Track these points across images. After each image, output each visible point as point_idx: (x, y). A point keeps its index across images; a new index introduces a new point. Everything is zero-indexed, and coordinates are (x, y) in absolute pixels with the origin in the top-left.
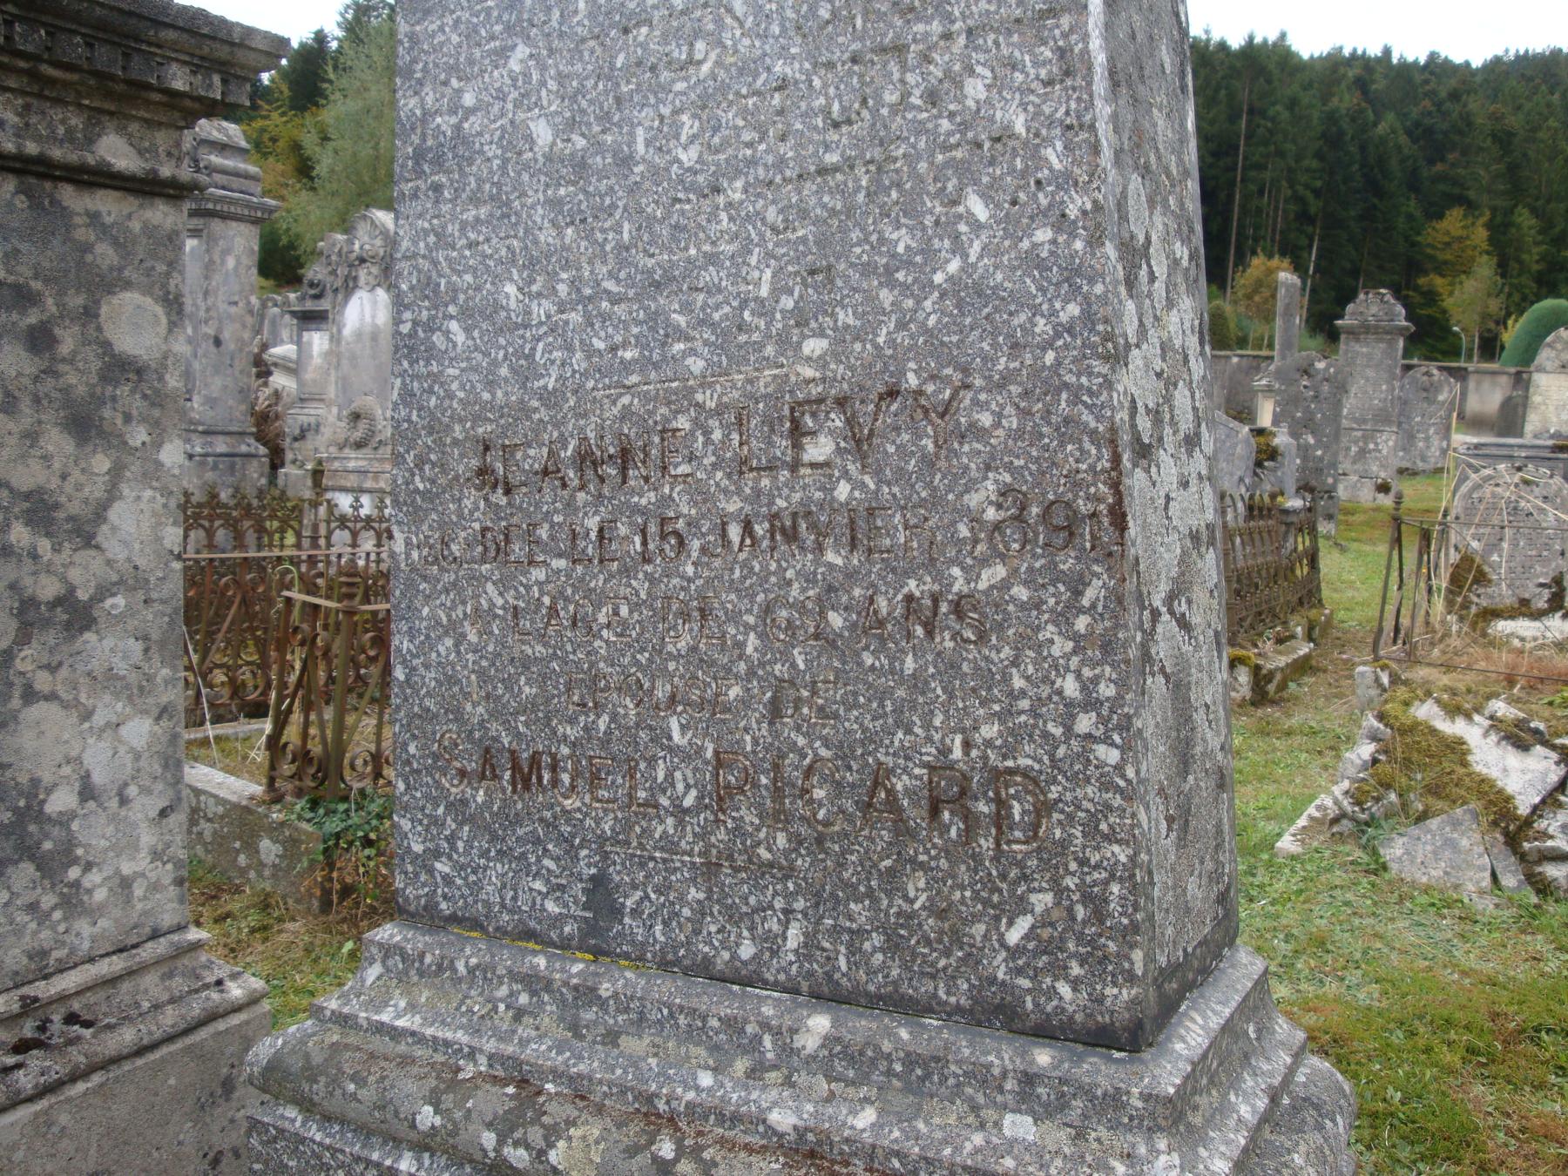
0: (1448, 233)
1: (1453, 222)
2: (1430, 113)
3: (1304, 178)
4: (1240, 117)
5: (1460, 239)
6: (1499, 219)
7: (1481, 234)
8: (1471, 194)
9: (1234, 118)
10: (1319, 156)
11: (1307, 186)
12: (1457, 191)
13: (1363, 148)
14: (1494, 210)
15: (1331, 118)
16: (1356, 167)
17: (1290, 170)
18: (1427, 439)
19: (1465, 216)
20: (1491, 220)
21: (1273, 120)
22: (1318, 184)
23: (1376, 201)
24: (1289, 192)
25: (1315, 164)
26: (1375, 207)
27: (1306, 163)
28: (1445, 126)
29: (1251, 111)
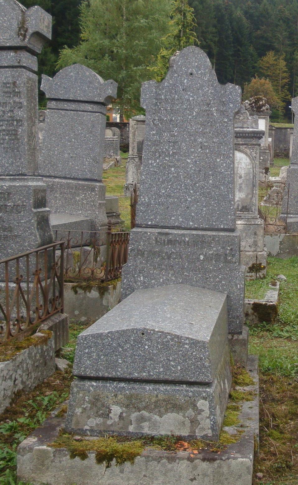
0: (268, 62)
1: (270, 57)
3: (210, 37)
5: (273, 65)
6: (289, 56)
7: (282, 64)
8: (276, 45)
10: (215, 26)
11: (211, 40)
12: (268, 44)
13: (231, 23)
14: (286, 52)
19: (275, 55)
20: (285, 57)
23: (239, 47)
25: (214, 30)
26: (239, 50)
28: (257, 14)
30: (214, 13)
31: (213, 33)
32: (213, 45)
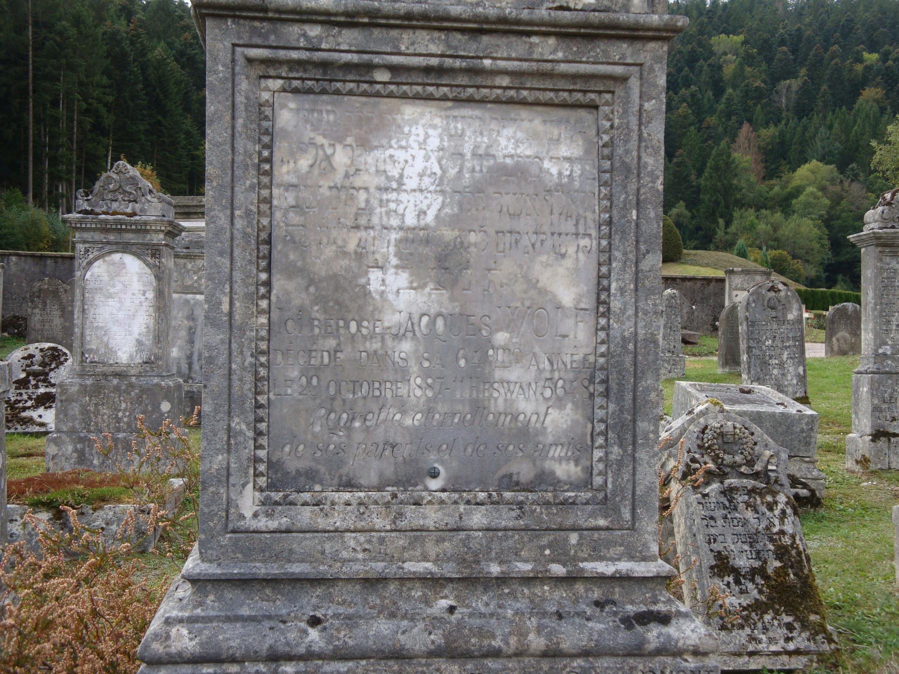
2: (191, 44)
3: (97, 93)
4: (26, 28)
9: (20, 29)
10: (107, 72)
11: (100, 101)
13: (143, 69)
15: (113, 38)
16: (141, 86)
17: (81, 84)
18: (781, 365)
21: (60, 34)
22: (110, 99)
23: (160, 118)
24: (84, 106)
25: (105, 80)
26: (159, 123)
27: (97, 78)
29: (36, 24)
30: (105, 48)
31: (104, 87)
32: (103, 110)
